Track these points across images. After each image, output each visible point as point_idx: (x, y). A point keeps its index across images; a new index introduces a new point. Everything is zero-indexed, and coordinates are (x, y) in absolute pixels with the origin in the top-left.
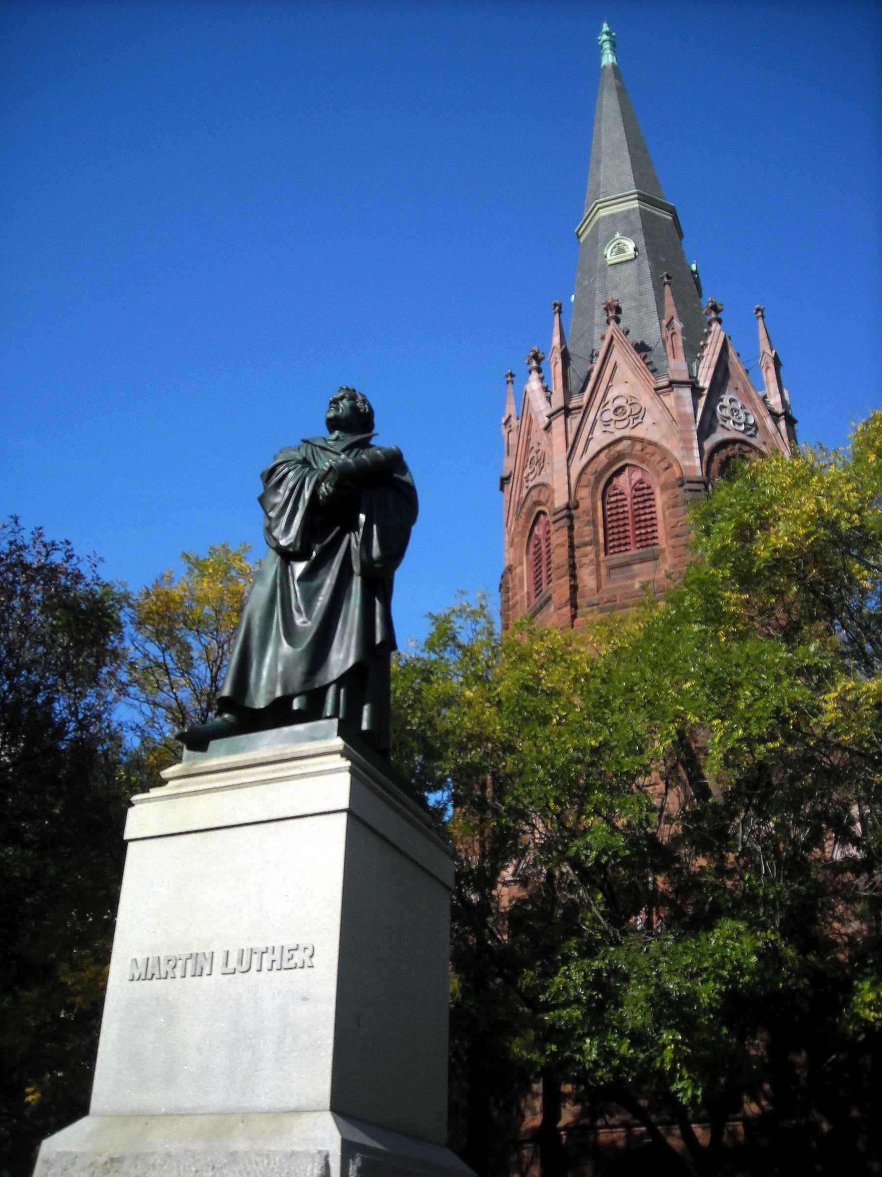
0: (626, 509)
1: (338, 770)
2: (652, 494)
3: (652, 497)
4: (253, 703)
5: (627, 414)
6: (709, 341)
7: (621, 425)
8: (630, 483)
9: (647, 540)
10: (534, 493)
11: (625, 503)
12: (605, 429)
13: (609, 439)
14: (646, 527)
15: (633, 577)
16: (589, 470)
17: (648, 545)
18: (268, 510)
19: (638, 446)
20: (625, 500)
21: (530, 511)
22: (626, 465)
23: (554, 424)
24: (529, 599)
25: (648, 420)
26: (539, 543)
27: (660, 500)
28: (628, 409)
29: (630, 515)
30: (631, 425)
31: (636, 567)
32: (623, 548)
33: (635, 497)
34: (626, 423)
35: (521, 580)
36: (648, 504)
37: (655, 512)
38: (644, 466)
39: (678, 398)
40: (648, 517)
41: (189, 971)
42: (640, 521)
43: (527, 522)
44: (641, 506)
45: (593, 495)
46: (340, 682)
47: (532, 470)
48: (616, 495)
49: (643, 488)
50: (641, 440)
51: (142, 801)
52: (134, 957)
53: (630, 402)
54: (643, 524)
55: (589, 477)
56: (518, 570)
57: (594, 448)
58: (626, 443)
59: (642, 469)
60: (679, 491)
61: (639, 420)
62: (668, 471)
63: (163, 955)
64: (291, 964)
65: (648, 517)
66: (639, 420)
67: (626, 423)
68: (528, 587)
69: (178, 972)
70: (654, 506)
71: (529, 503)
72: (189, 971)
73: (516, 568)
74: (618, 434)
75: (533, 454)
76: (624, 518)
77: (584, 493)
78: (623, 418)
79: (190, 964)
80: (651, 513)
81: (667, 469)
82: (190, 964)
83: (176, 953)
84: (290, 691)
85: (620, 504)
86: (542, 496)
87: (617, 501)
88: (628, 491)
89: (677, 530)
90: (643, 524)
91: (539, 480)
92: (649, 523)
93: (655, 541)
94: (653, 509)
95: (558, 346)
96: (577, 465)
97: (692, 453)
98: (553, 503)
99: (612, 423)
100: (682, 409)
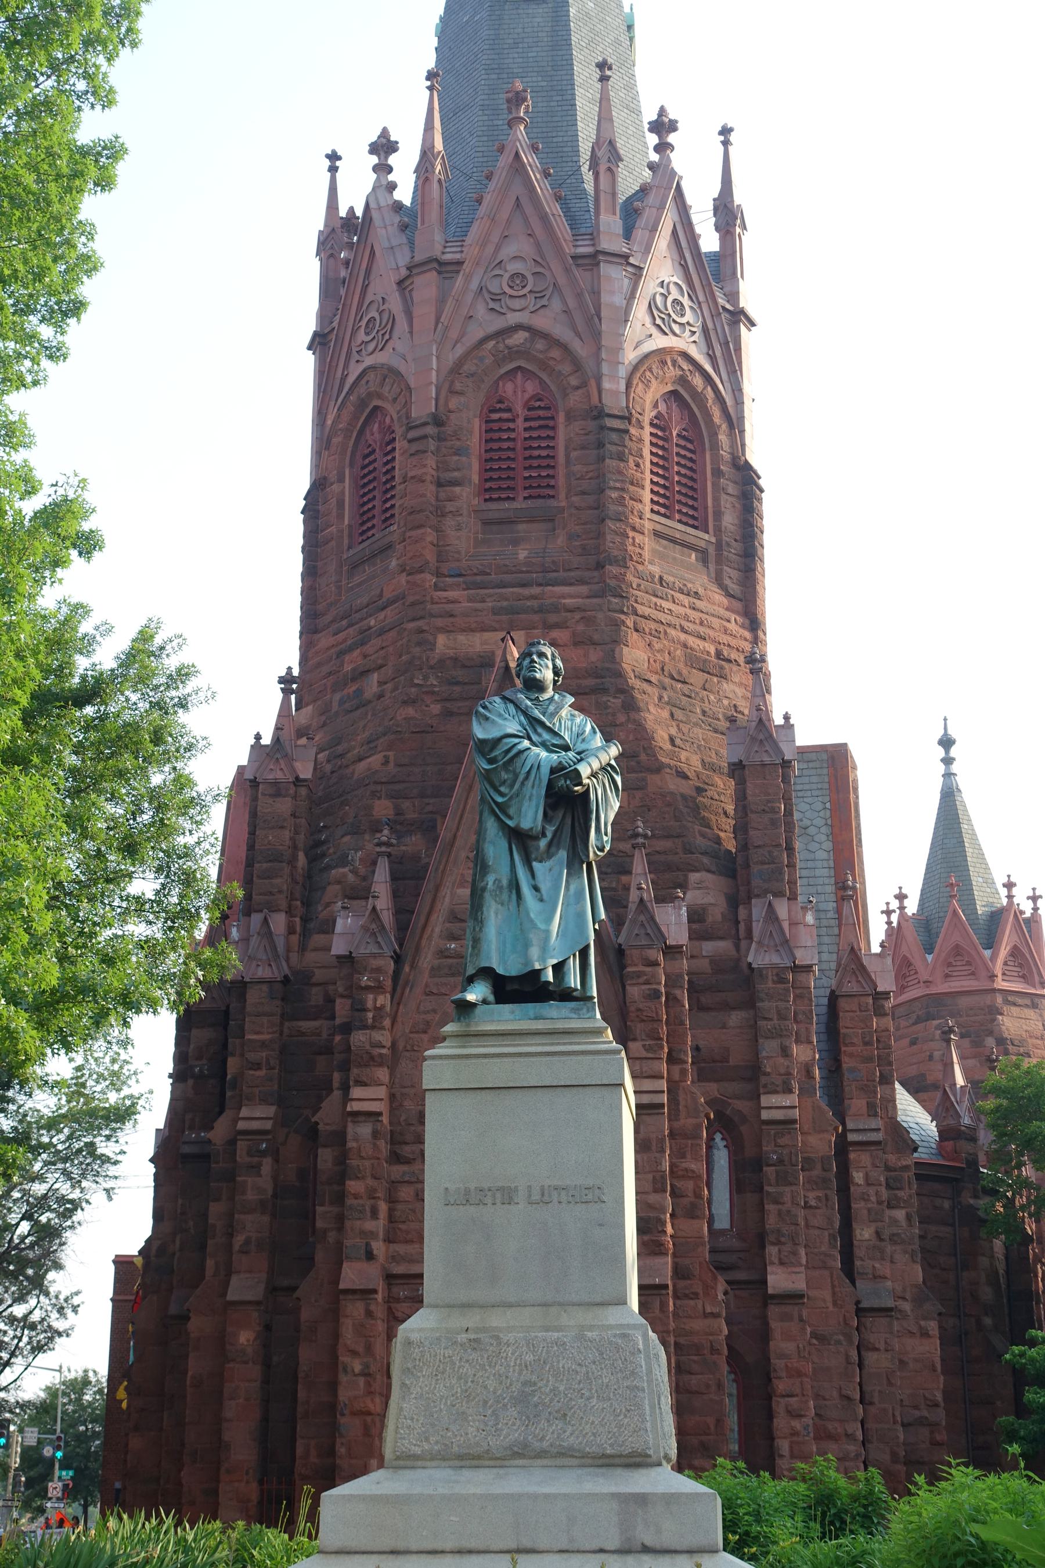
3: (551, 423)
7: (517, 304)
10: (371, 376)
11: (511, 425)
12: (492, 305)
13: (498, 323)
15: (515, 542)
17: (539, 497)
18: (498, 784)
19: (540, 345)
20: (513, 420)
21: (362, 403)
24: (350, 536)
26: (374, 451)
28: (530, 278)
29: (519, 445)
31: (521, 527)
33: (526, 420)
35: (341, 504)
37: (553, 448)
38: (544, 376)
40: (544, 453)
41: (498, 1201)
42: (531, 457)
43: (355, 417)
44: (535, 434)
48: (500, 410)
49: (540, 408)
50: (545, 336)
52: (447, 1185)
54: (535, 463)
56: (336, 488)
59: (542, 382)
63: (472, 1186)
65: (544, 453)
66: (544, 302)
67: (522, 303)
69: (489, 1200)
70: (553, 438)
71: (362, 390)
72: (498, 1201)
73: (332, 484)
74: (513, 319)
75: (373, 313)
78: (521, 293)
79: (498, 1195)
80: (548, 447)
82: (498, 1195)
83: (486, 1185)
85: (505, 426)
86: (387, 388)
87: (500, 420)
91: (381, 358)
92: (544, 463)
98: (407, 404)
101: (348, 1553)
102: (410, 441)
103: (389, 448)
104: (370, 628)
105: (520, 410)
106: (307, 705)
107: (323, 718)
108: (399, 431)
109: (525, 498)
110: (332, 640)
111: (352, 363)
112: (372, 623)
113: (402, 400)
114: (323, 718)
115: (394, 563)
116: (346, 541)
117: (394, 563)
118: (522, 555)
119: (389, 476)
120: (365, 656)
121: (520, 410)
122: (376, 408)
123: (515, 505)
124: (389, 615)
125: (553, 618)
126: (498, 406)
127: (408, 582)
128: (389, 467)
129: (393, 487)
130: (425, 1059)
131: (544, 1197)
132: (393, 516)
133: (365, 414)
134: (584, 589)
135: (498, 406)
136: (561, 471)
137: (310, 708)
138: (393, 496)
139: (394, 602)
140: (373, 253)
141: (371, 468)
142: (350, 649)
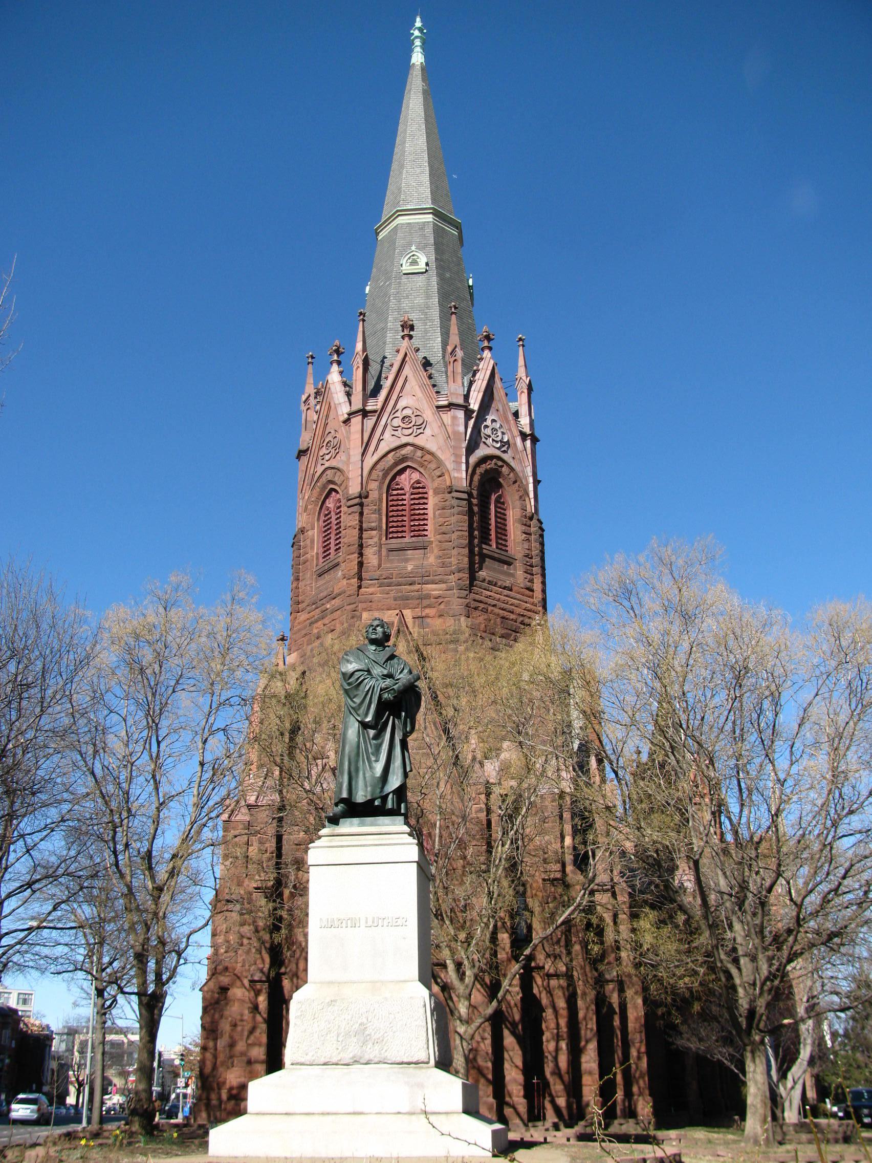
0: (405, 502)
1: (412, 844)
2: (426, 493)
3: (425, 496)
4: (355, 799)
5: (413, 423)
6: (480, 367)
8: (410, 482)
9: (419, 531)
10: (329, 472)
11: (404, 497)
13: (397, 443)
14: (419, 520)
15: (407, 560)
16: (380, 466)
17: (419, 536)
19: (419, 453)
20: (405, 495)
21: (324, 487)
22: (409, 467)
23: (352, 420)
24: (317, 558)
25: (428, 431)
26: (330, 513)
27: (432, 501)
28: (414, 419)
29: (407, 508)
30: (414, 434)
31: (410, 552)
32: (400, 535)
33: (412, 494)
34: (410, 431)
35: (312, 541)
36: (422, 501)
38: (421, 470)
39: (454, 418)
40: (422, 512)
44: (416, 502)
45: (380, 488)
46: (394, 792)
47: (328, 451)
48: (398, 489)
49: (419, 488)
50: (422, 449)
51: (314, 847)
53: (415, 414)
54: (417, 517)
55: (377, 473)
56: (310, 533)
57: (384, 448)
58: (409, 448)
60: (448, 496)
61: (421, 431)
62: (441, 478)
64: (397, 924)
65: (422, 512)
66: (421, 431)
67: (410, 431)
68: (318, 549)
69: (344, 925)
71: (324, 480)
72: (349, 925)
73: (308, 531)
74: (405, 440)
76: (403, 510)
77: (373, 485)
78: (409, 426)
79: (349, 922)
81: (440, 476)
82: (349, 922)
84: (374, 796)
85: (400, 498)
87: (398, 495)
88: (407, 488)
89: (444, 529)
90: (417, 517)
91: (333, 463)
93: (425, 533)
94: (425, 506)
95: (361, 353)
96: (370, 460)
97: (461, 467)
98: (346, 488)
99: (399, 429)
100: (456, 428)
101: (264, 1114)
102: (349, 507)
103: (338, 511)
104: (327, 609)
105: (407, 488)
106: (294, 652)
107: (302, 659)
108: (343, 501)
109: (412, 537)
110: (307, 616)
111: (319, 465)
112: (328, 606)
113: (344, 484)
114: (302, 659)
115: (340, 573)
116: (315, 562)
117: (340, 573)
118: (410, 568)
119: (338, 526)
120: (324, 625)
121: (407, 488)
122: (332, 490)
123: (406, 540)
124: (337, 602)
125: (426, 602)
126: (397, 487)
127: (347, 583)
128: (338, 521)
129: (340, 532)
130: (309, 849)
131: (375, 923)
132: (340, 548)
133: (326, 493)
134: (443, 586)
135: (397, 487)
136: (429, 522)
137: (296, 653)
138: (340, 537)
139: (340, 595)
140: (330, 407)
141: (329, 522)
142: (316, 621)
